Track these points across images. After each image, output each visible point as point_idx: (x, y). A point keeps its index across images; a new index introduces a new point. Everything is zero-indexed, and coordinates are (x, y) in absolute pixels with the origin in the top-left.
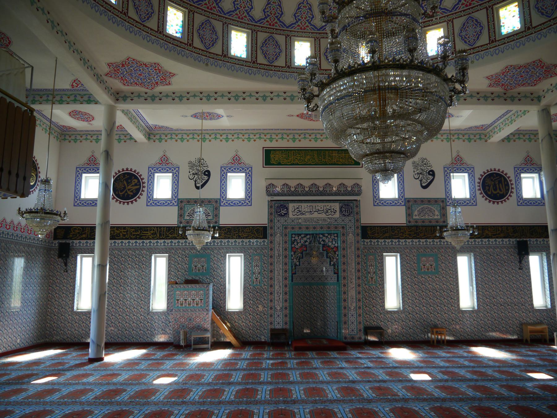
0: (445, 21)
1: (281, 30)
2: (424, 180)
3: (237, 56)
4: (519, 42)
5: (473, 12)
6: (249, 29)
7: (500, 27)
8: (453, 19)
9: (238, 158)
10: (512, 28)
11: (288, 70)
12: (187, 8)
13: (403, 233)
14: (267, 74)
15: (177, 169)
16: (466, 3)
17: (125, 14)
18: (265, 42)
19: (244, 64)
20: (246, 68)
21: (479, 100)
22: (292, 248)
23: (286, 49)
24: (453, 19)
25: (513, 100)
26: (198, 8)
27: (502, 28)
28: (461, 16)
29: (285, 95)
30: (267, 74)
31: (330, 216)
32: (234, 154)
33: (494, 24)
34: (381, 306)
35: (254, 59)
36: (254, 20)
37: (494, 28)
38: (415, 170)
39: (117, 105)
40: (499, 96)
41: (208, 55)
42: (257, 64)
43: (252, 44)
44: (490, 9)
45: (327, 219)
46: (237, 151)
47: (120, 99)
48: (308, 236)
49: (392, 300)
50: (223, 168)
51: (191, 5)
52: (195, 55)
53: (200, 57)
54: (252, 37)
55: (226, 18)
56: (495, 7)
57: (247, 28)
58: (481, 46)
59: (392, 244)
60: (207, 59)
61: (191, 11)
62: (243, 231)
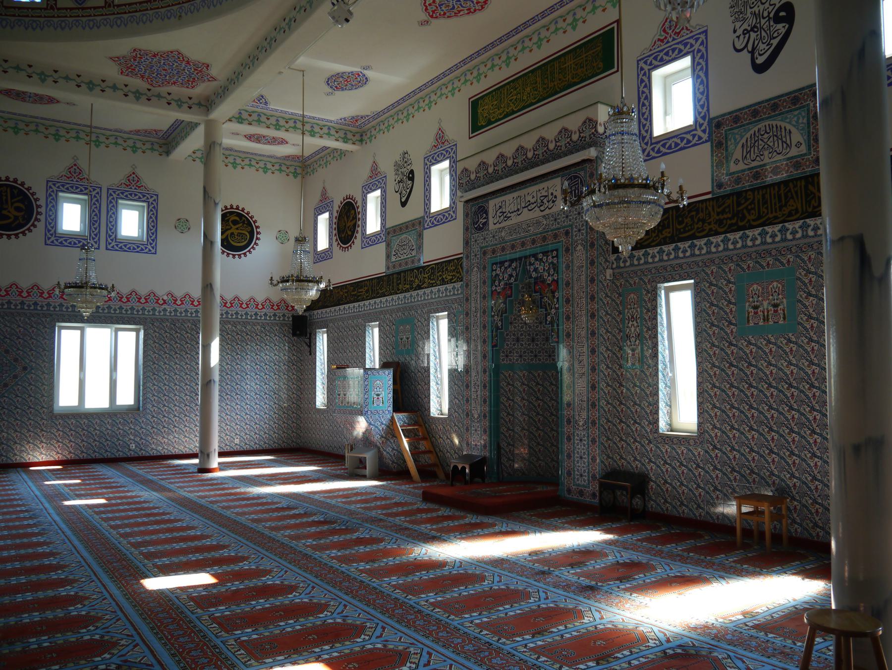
2: (762, 46)
13: (703, 221)
17: (52, 8)
22: (492, 292)
31: (547, 212)
34: (650, 423)
38: (738, 24)
45: (541, 219)
48: (514, 265)
49: (681, 407)
59: (677, 257)
62: (447, 269)
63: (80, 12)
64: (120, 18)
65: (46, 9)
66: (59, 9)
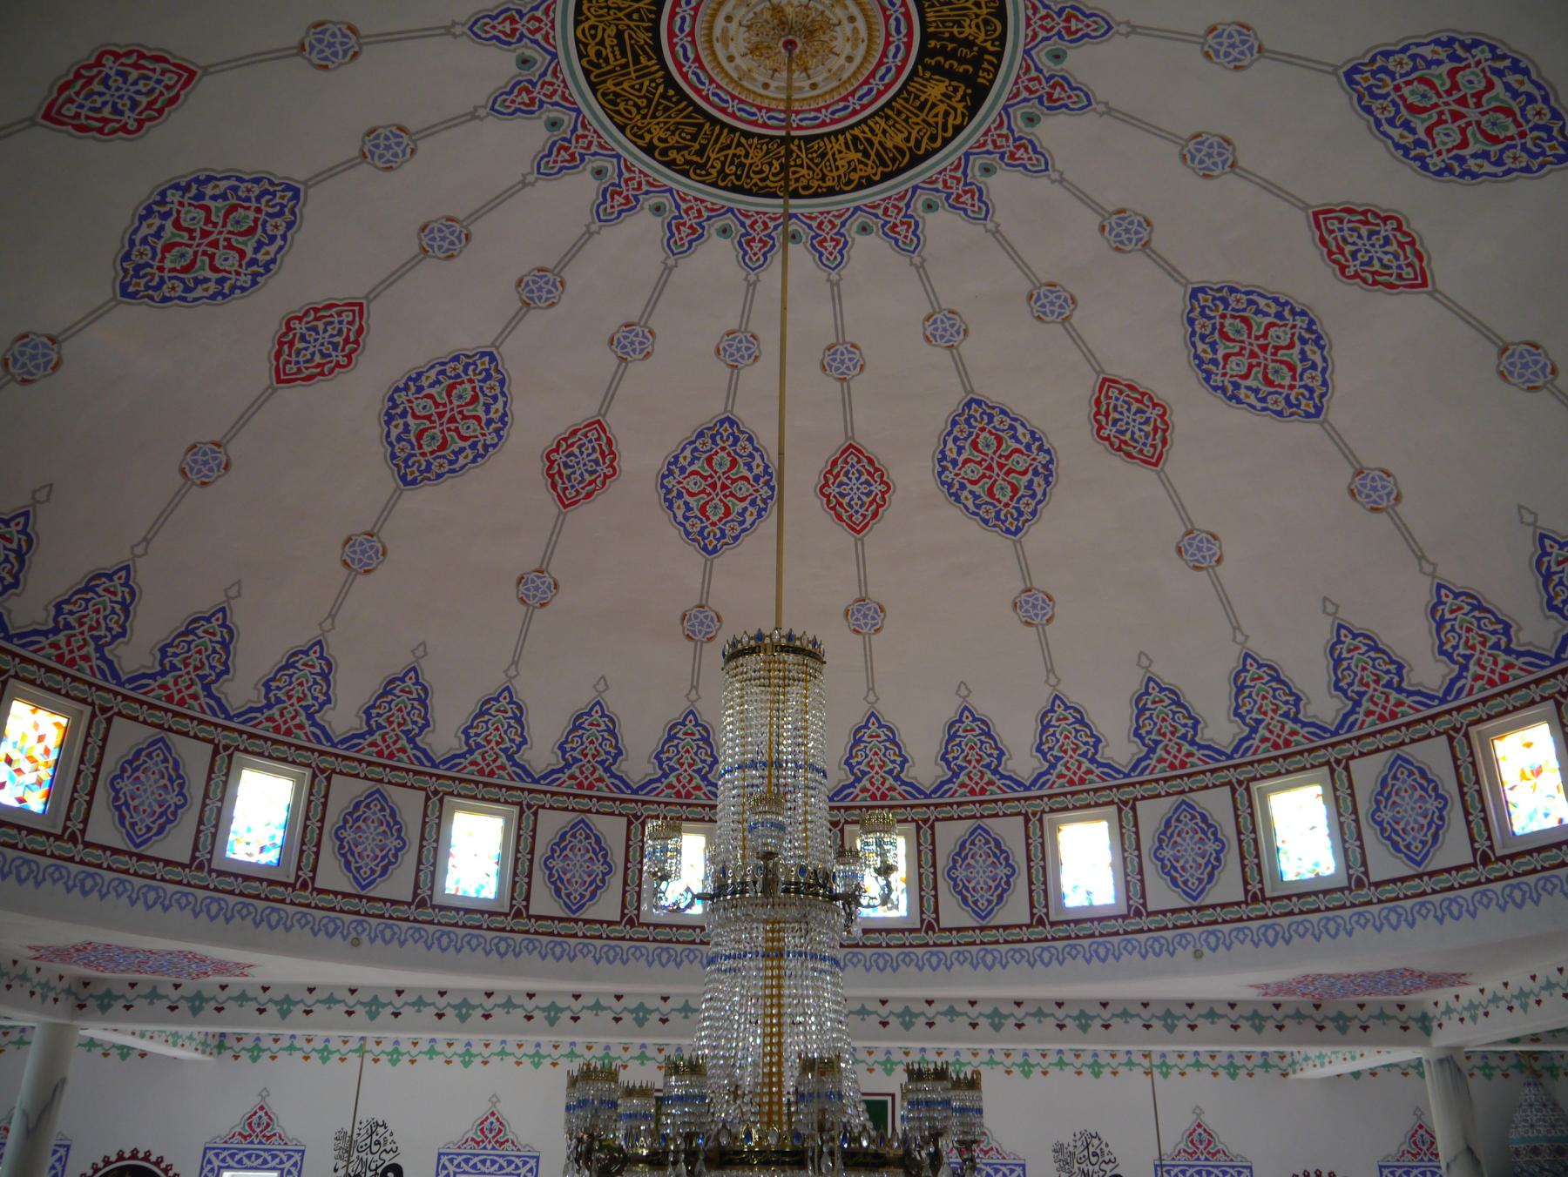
0: (1111, 803)
1: (614, 800)
3: (464, 898)
4: (1333, 919)
5: (1192, 790)
6: (513, 803)
7: (1274, 851)
8: (1136, 799)
9: (496, 1125)
10: (1311, 867)
11: (628, 931)
12: (309, 766)
14: (558, 950)
15: (297, 1157)
16: (1170, 758)
17: (73, 838)
18: (561, 843)
19: (485, 920)
20: (490, 935)
21: (1235, 1027)
23: (627, 860)
24: (1136, 799)
25: (1343, 1030)
26: (345, 758)
27: (1282, 856)
28: (1159, 796)
29: (618, 1006)
30: (558, 950)
32: (483, 1109)
33: (1255, 841)
35: (520, 903)
36: (529, 774)
37: (1258, 856)
39: (75, 1023)
40: (1299, 1016)
41: (364, 906)
42: (529, 917)
43: (517, 851)
44: (1241, 790)
46: (494, 1100)
47: (92, 1003)
50: (444, 1160)
51: (322, 753)
52: (319, 914)
53: (333, 920)
54: (519, 828)
55: (439, 777)
56: (1254, 786)
57: (506, 802)
58: (1223, 906)
60: (360, 923)
61: (323, 771)
63: (133, 864)
64: (218, 900)
65: (58, 838)
66: (87, 845)
